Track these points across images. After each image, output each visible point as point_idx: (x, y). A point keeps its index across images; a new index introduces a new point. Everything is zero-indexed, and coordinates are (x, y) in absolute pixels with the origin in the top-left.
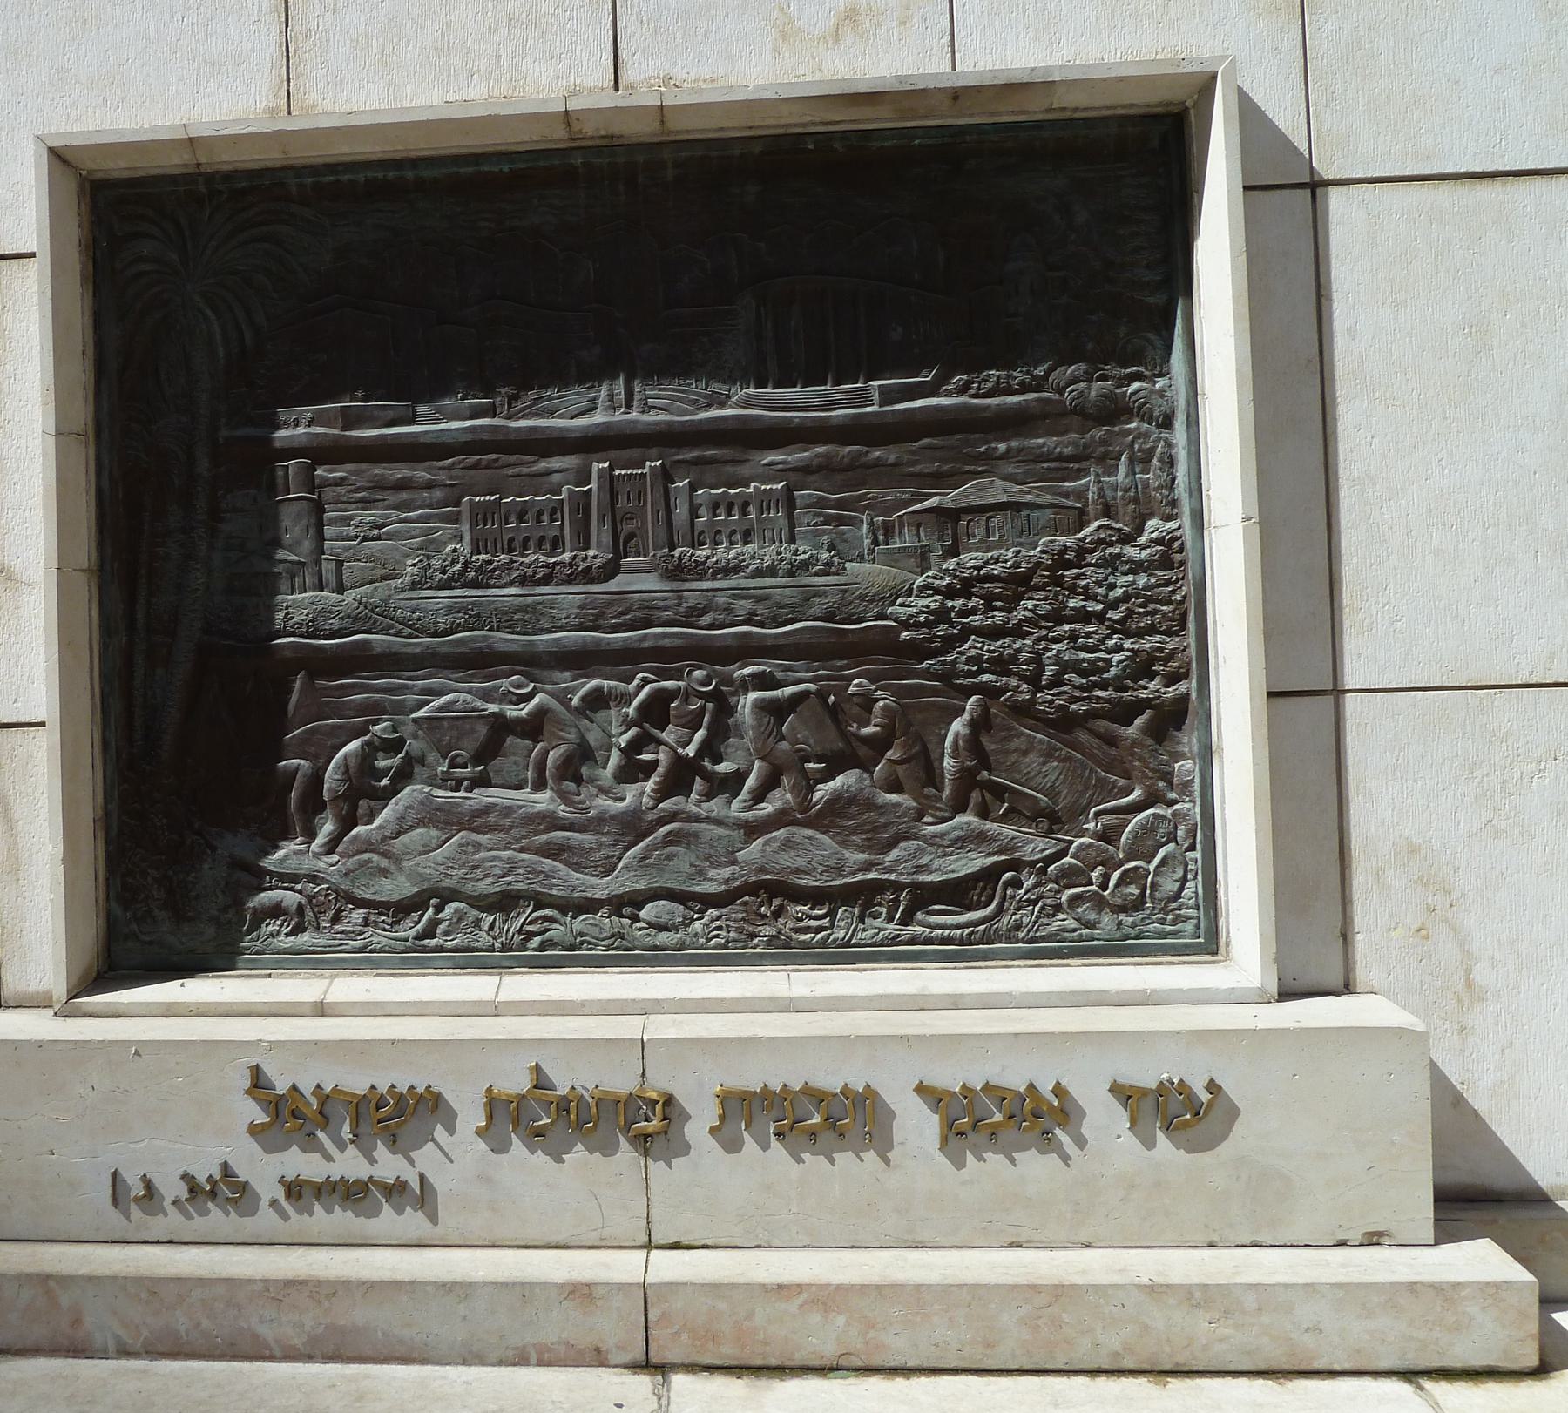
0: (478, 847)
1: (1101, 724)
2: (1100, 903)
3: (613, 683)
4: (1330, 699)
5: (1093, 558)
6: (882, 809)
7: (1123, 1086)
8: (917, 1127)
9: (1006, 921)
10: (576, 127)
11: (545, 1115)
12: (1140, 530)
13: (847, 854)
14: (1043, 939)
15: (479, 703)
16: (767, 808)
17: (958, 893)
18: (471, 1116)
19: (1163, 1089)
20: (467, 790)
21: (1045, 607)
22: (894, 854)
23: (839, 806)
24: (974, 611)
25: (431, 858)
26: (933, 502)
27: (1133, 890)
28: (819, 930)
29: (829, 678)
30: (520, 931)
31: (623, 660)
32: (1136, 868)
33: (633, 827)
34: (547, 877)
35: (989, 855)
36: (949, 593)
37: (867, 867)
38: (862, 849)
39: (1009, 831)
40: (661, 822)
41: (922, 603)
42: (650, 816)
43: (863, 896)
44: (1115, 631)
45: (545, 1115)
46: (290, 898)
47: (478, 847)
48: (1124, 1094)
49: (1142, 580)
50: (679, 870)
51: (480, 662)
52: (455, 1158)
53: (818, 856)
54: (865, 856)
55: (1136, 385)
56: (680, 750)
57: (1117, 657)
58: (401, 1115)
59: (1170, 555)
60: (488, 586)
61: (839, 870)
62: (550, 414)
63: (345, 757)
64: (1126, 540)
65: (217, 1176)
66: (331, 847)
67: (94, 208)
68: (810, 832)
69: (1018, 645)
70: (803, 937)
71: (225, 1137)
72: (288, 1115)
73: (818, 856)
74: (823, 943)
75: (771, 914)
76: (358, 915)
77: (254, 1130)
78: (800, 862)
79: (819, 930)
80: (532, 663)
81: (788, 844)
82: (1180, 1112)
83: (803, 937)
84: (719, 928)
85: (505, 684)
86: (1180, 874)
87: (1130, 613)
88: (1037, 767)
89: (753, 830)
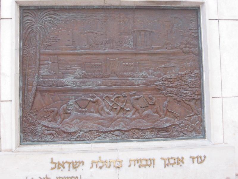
0: (87, 123)
1: (187, 102)
2: (188, 131)
3: (110, 95)
4: (220, 99)
5: (186, 76)
6: (153, 116)
7: (192, 157)
9: (173, 134)
10: (105, 2)
11: (102, 165)
12: (193, 72)
13: (148, 123)
14: (179, 137)
15: (87, 98)
16: (135, 116)
17: (165, 130)
19: (197, 158)
20: (84, 113)
21: (179, 83)
22: (156, 123)
23: (148, 116)
24: (168, 84)
26: (162, 66)
27: (192, 129)
28: (143, 136)
29: (145, 95)
30: (94, 137)
32: (193, 125)
33: (112, 120)
34: (99, 128)
35: (170, 124)
36: (164, 81)
37: (151, 125)
38: (151, 123)
39: (173, 120)
40: (118, 118)
41: (160, 82)
42: (116, 117)
44: (189, 87)
46: (54, 132)
47: (86, 122)
48: (193, 158)
49: (193, 79)
54: (150, 124)
55: (193, 49)
56: (121, 106)
57: (190, 92)
60: (89, 78)
61: (147, 126)
62: (99, 50)
63: (63, 107)
64: (191, 73)
65: (45, 177)
66: (61, 123)
67: (20, 10)
68: (142, 120)
69: (175, 90)
70: (141, 137)
74: (144, 138)
76: (65, 135)
77: (52, 169)
78: (140, 125)
79: (143, 136)
81: (139, 122)
83: (141, 137)
84: (127, 136)
85: (91, 95)
86: (199, 126)
87: (192, 85)
88: (177, 109)
89: (134, 119)
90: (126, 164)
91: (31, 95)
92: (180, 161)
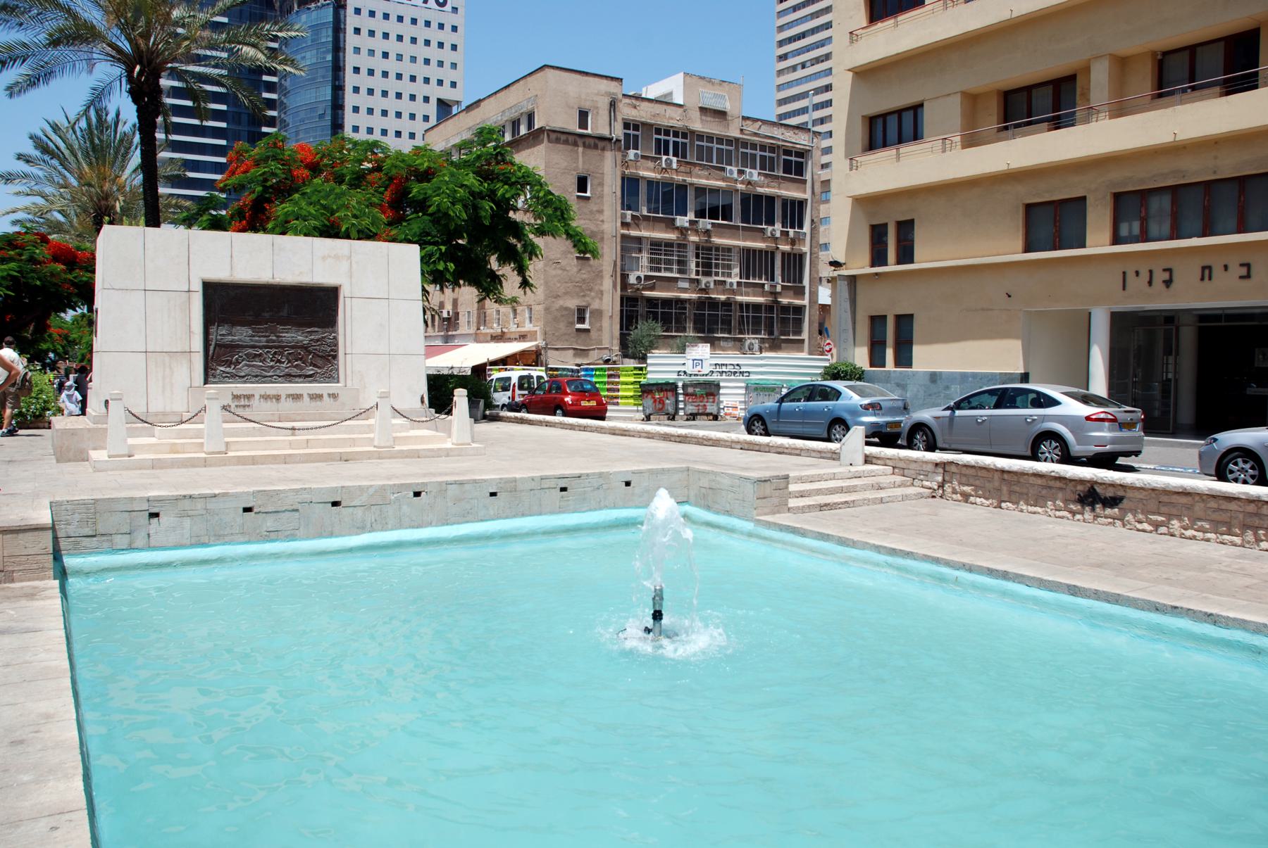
8: (306, 398)
11: (266, 397)
17: (310, 376)
18: (257, 397)
25: (245, 371)
31: (271, 347)
33: (272, 367)
43: (300, 376)
45: (266, 397)
50: (278, 372)
51: (253, 347)
52: (255, 402)
53: (294, 371)
58: (249, 397)
59: (335, 338)
71: (228, 400)
72: (236, 397)
73: (294, 371)
75: (289, 377)
80: (261, 348)
82: (334, 396)
88: (320, 362)
90: (283, 397)
91: (212, 348)
92: (320, 397)
